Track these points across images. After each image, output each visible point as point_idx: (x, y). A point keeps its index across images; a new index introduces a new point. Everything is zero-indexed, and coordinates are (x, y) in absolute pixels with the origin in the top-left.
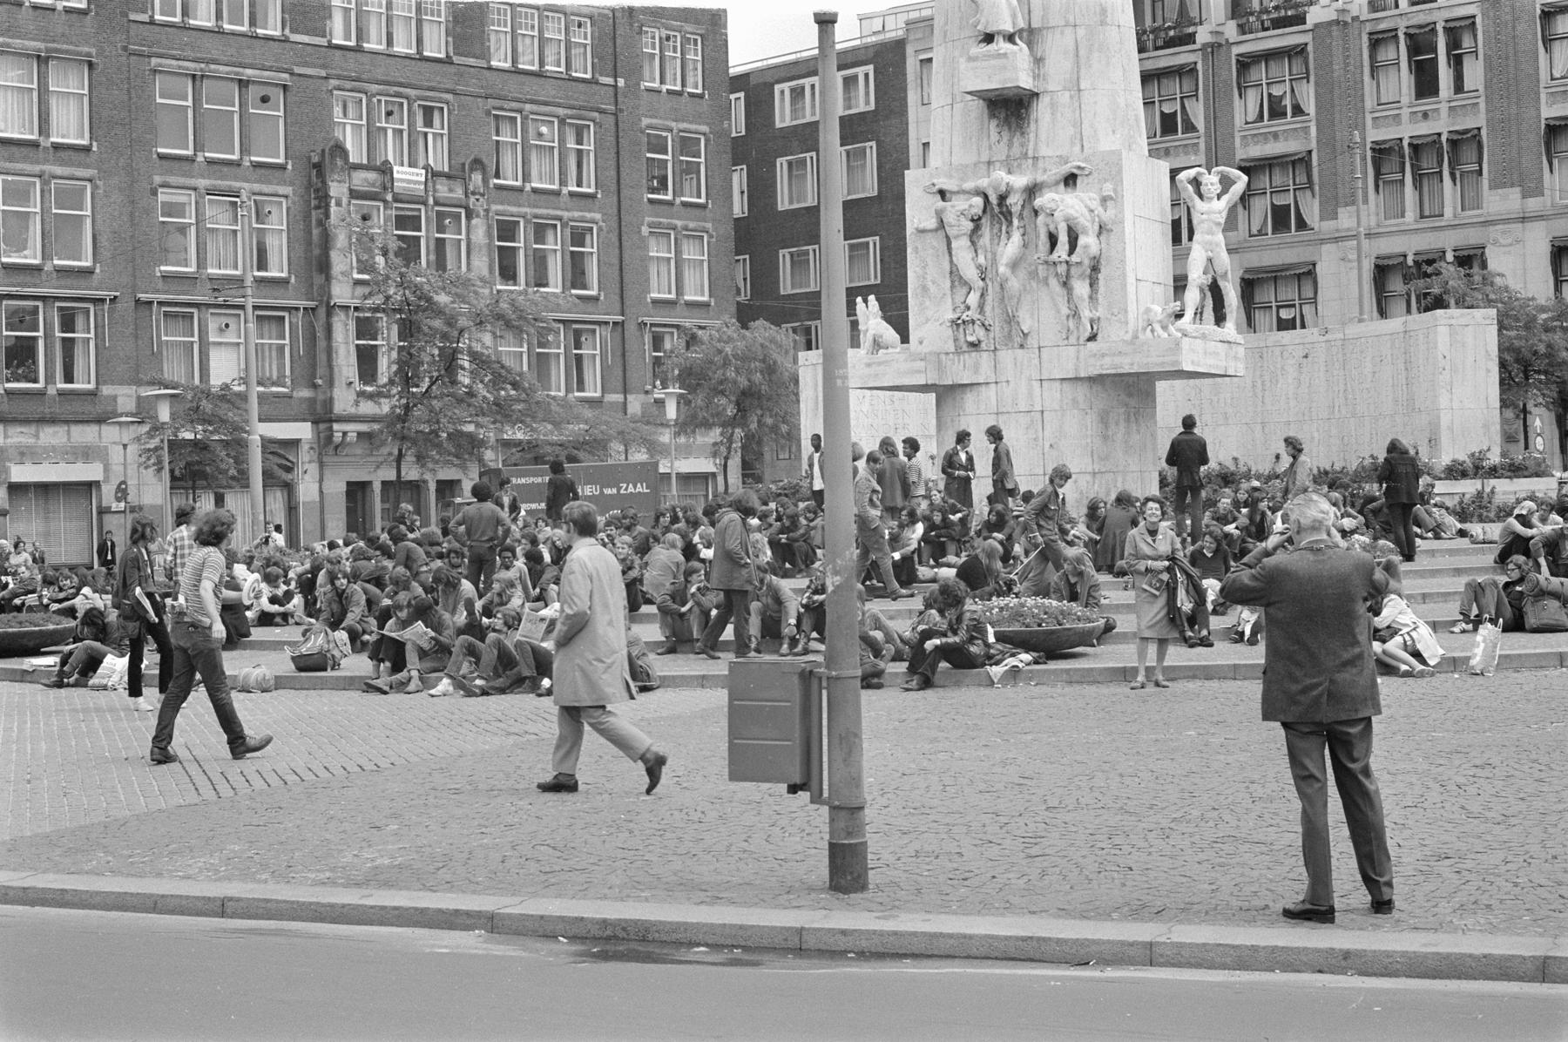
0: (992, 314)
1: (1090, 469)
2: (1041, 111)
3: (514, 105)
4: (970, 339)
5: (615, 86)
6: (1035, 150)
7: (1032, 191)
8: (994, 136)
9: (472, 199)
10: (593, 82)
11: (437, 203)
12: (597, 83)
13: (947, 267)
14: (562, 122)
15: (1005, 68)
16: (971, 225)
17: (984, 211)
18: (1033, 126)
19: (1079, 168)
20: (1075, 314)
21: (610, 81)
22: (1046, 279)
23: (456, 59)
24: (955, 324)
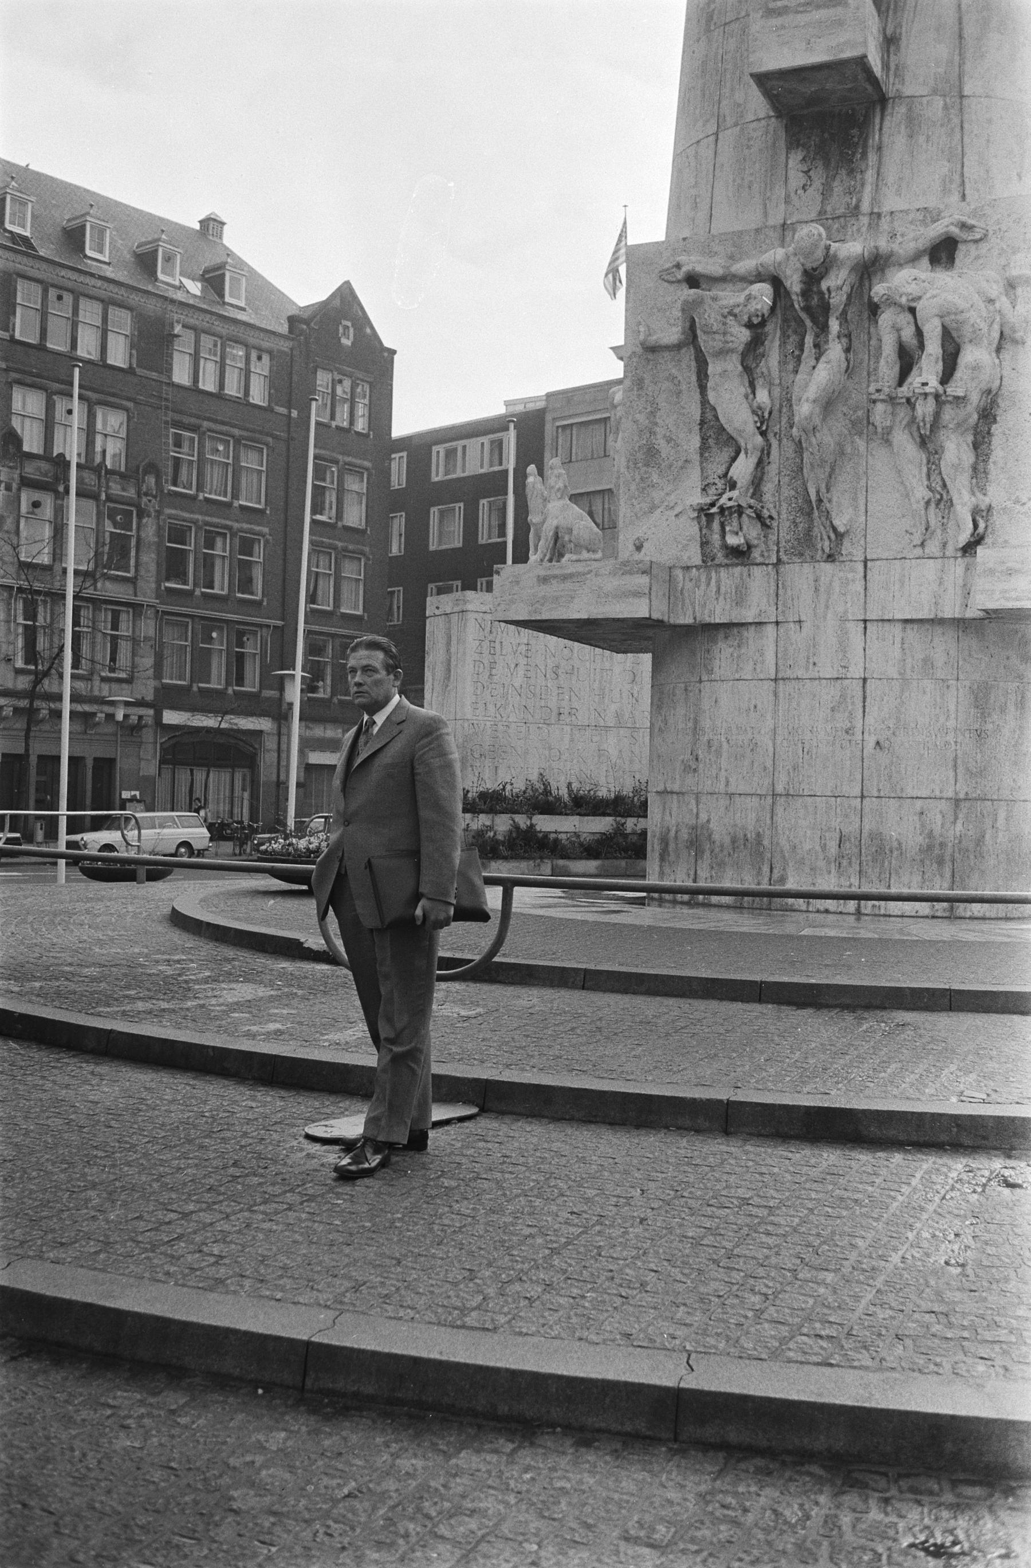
0: (777, 497)
1: (950, 794)
2: (891, 132)
3: (193, 420)
4: (732, 540)
5: (289, 416)
6: (875, 201)
7: (871, 267)
8: (796, 178)
9: (145, 499)
10: (269, 409)
11: (109, 498)
12: (272, 411)
13: (695, 411)
14: (238, 441)
15: (840, 23)
16: (744, 335)
17: (773, 309)
18: (872, 157)
19: (963, 226)
20: (941, 500)
21: (283, 410)
22: (888, 431)
23: (139, 371)
24: (704, 513)
